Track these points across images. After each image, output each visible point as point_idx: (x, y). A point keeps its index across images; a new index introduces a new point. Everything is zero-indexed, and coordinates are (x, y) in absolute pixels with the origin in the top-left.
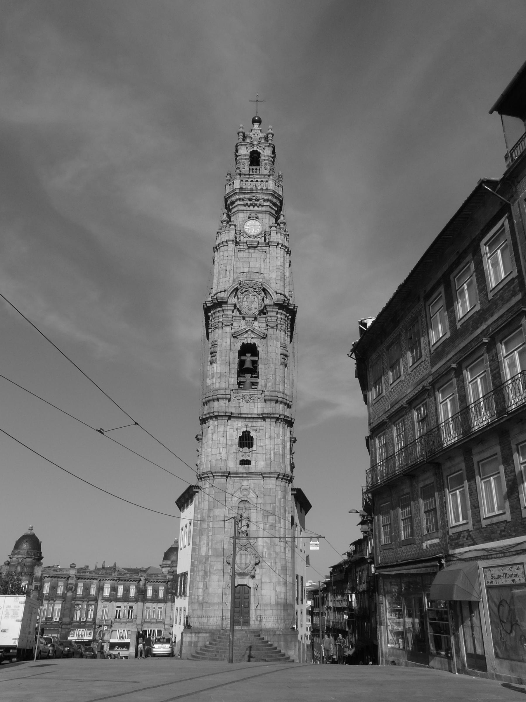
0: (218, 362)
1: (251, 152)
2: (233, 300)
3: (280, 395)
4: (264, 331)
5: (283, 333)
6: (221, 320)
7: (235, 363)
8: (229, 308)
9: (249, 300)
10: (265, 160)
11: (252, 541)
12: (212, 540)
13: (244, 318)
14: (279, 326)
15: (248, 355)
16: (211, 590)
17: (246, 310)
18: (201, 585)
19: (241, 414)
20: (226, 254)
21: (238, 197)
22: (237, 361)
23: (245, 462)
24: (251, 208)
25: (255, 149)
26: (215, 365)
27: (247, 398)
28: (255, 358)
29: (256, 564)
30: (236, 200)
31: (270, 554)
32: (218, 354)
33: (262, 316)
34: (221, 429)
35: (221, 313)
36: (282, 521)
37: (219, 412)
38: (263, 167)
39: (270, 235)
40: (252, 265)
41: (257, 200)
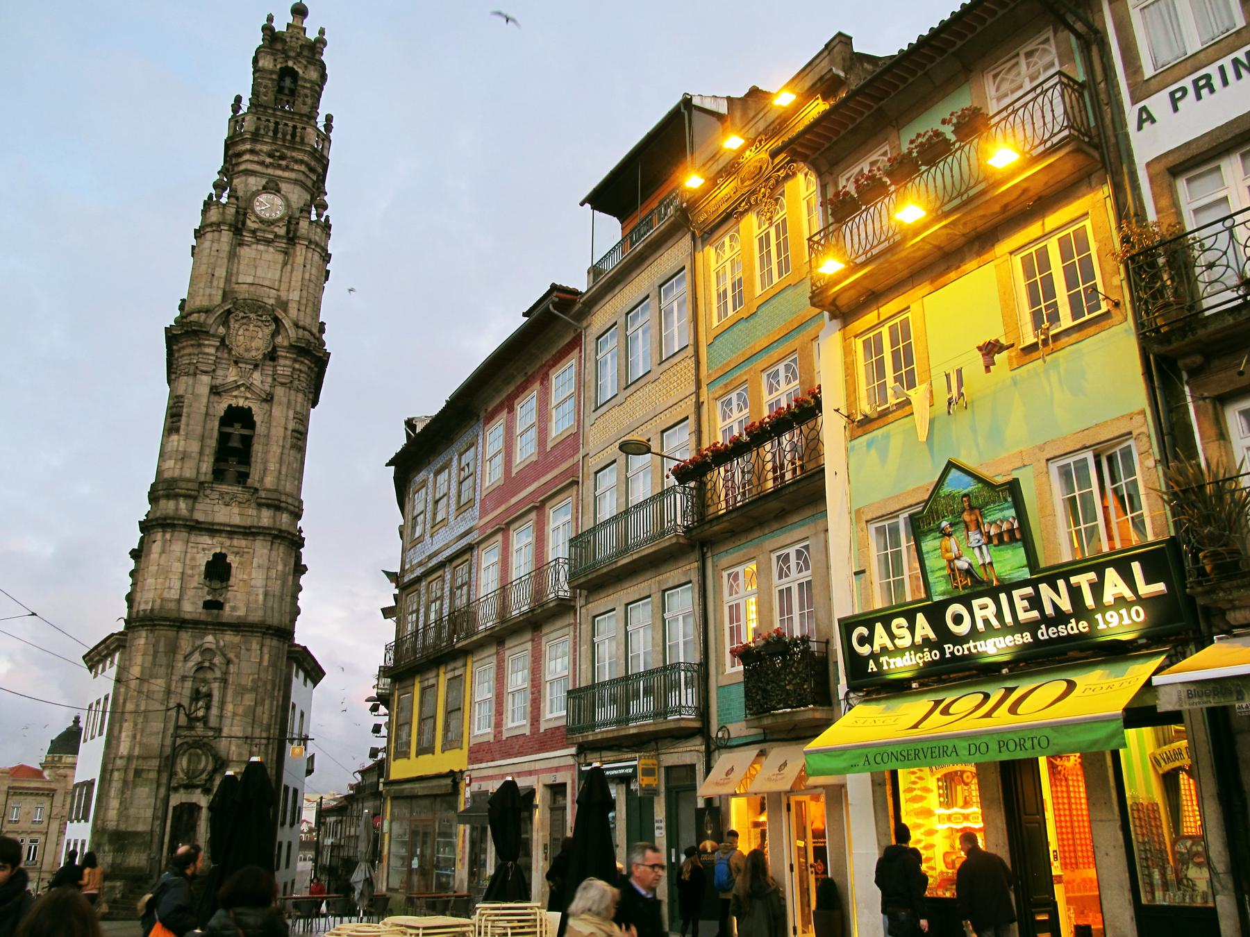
0: (182, 432)
2: (222, 330)
3: (283, 498)
4: (267, 388)
5: (301, 395)
7: (211, 438)
9: (247, 333)
12: (143, 731)
13: (236, 363)
14: (296, 382)
15: (238, 426)
16: (132, 811)
18: (114, 803)
19: (213, 524)
20: (215, 246)
21: (248, 147)
22: (216, 434)
25: (290, 64)
26: (175, 437)
27: (227, 498)
28: (246, 432)
30: (244, 152)
31: (240, 755)
32: (184, 420)
33: (268, 363)
34: (177, 547)
36: (267, 702)
38: (300, 100)
40: (260, 273)
41: (283, 157)
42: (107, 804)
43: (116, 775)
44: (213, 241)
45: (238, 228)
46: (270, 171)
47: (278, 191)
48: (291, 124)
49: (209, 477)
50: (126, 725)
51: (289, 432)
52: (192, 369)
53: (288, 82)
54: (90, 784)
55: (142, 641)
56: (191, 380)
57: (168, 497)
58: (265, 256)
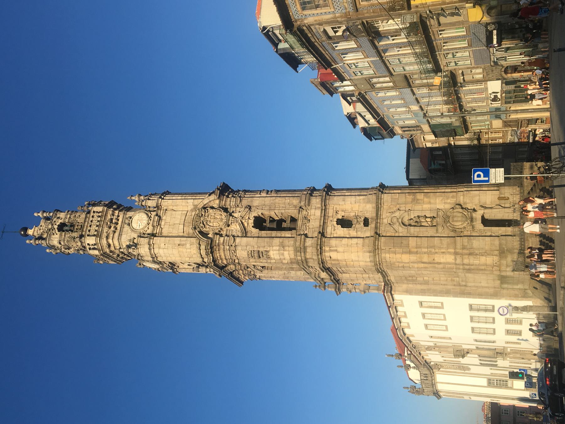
0: (268, 249)
1: (59, 231)
2: (210, 236)
6: (228, 247)
8: (217, 239)
10: (70, 217)
11: (441, 213)
13: (229, 226)
17: (221, 224)
18: (483, 259)
19: (320, 226)
20: (162, 245)
21: (105, 239)
23: (366, 222)
25: (56, 227)
26: (271, 254)
29: (462, 208)
31: (453, 197)
32: (261, 249)
35: (222, 247)
37: (317, 245)
39: (149, 207)
42: (483, 265)
43: (466, 261)
44: (159, 248)
45: (153, 235)
46: (119, 228)
47: (131, 218)
48: (91, 219)
49: (294, 231)
50: (437, 260)
51: (268, 195)
52: (233, 248)
54: (471, 308)
55: (388, 255)
56: (239, 248)
57: (305, 252)
58: (168, 220)
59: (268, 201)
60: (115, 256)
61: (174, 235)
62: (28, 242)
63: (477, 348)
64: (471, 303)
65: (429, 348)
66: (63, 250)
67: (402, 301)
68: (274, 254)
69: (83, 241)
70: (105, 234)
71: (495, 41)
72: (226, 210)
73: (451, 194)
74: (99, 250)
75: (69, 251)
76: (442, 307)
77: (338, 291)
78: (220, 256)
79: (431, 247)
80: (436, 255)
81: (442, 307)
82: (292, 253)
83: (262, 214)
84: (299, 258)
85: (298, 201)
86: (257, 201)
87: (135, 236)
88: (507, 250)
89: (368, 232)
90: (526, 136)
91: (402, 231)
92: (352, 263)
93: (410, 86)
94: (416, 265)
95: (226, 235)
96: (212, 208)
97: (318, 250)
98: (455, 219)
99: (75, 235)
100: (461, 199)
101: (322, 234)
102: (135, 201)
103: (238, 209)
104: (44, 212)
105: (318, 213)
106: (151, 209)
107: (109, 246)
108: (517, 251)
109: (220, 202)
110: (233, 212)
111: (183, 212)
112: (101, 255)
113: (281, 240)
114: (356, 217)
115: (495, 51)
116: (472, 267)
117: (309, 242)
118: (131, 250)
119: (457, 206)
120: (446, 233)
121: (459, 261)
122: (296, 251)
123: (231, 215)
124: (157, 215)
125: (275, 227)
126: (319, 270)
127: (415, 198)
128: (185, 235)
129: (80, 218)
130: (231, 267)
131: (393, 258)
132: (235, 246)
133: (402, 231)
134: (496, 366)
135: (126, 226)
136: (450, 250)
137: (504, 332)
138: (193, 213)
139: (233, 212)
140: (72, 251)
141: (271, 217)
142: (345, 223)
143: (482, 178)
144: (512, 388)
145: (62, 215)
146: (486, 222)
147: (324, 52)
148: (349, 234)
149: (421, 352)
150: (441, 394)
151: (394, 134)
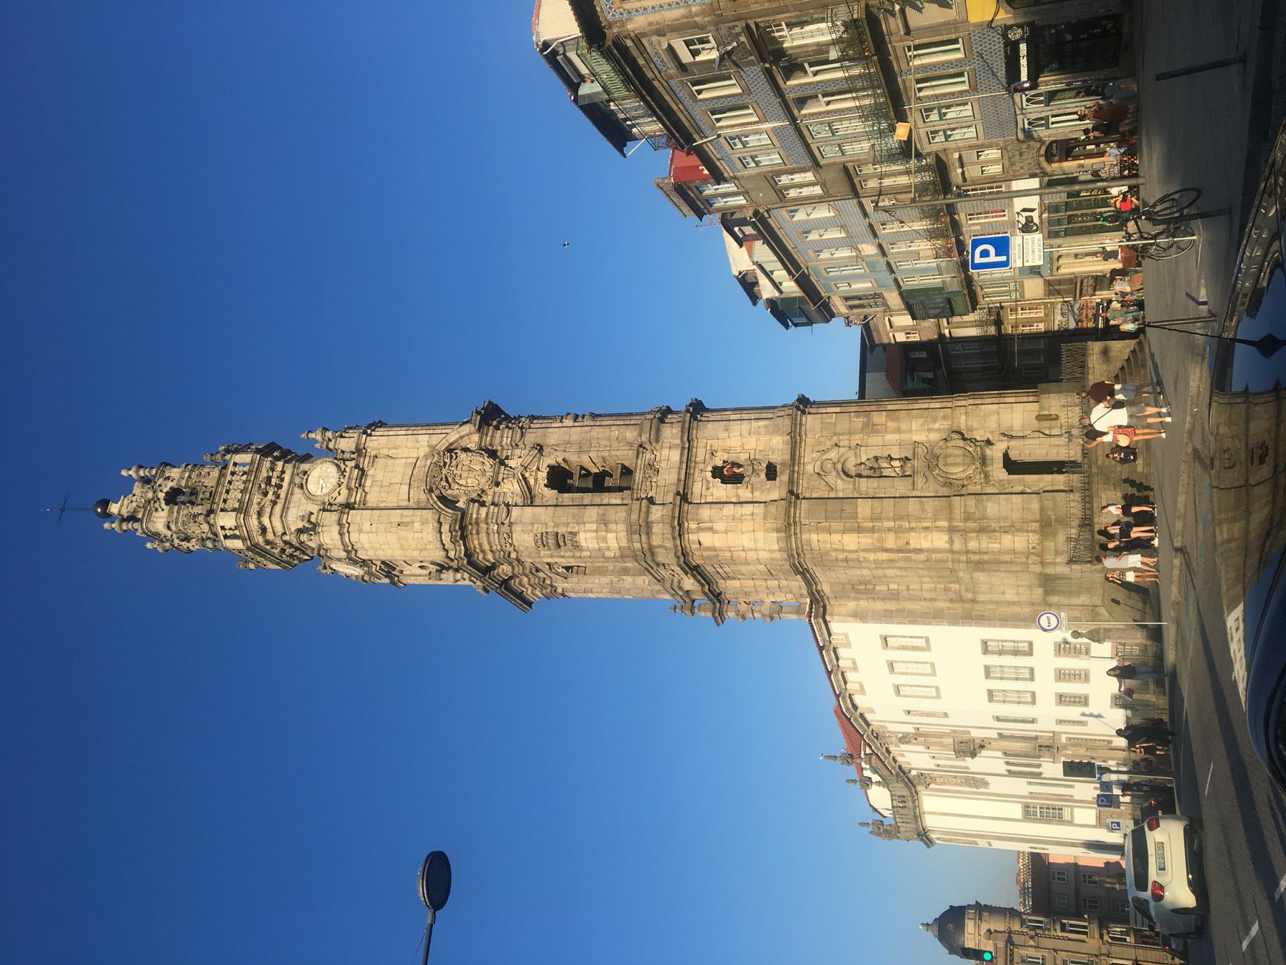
2: (460, 505)
10: (189, 477)
11: (920, 451)
13: (497, 484)
17: (483, 480)
18: (1007, 541)
19: (679, 480)
20: (366, 526)
21: (255, 516)
23: (771, 473)
24: (283, 493)
25: (161, 495)
29: (964, 439)
31: (944, 418)
32: (562, 530)
35: (483, 526)
37: (673, 517)
39: (343, 452)
43: (973, 545)
44: (360, 531)
45: (349, 506)
46: (283, 496)
47: (305, 473)
48: (229, 477)
49: (627, 493)
50: (913, 544)
52: (505, 529)
53: (182, 498)
55: (814, 537)
57: (648, 534)
58: (379, 476)
59: (576, 433)
60: (276, 551)
61: (389, 505)
62: (106, 526)
63: (1000, 735)
64: (986, 637)
65: (905, 739)
66: (176, 542)
67: (846, 636)
68: (587, 539)
69: (212, 522)
70: (255, 508)
71: (1024, 76)
72: (492, 454)
73: (942, 413)
74: (244, 540)
75: (189, 545)
76: (927, 648)
77: (719, 617)
78: (480, 545)
79: (901, 518)
80: (913, 534)
81: (927, 648)
82: (623, 535)
83: (564, 460)
84: (637, 545)
85: (636, 433)
86: (554, 435)
87: (315, 509)
88: (1056, 520)
89: (775, 491)
90: (1090, 315)
91: (842, 487)
92: (743, 554)
93: (856, 195)
94: (871, 556)
95: (493, 504)
96: (466, 450)
97: (673, 528)
98: (950, 460)
99: (197, 510)
100: (962, 422)
101: (684, 497)
102: (316, 441)
103: (517, 452)
104: (140, 467)
105: (675, 456)
106: (347, 456)
107: (264, 530)
108: (1077, 522)
109: (481, 438)
110: (507, 458)
111: (410, 461)
112: (248, 549)
113: (601, 510)
114: (752, 462)
115: (1025, 103)
116: (986, 557)
117: (656, 513)
118: (304, 537)
119: (955, 436)
120: (933, 488)
121: (958, 545)
122: (631, 531)
123: (502, 463)
124: (357, 466)
125: (591, 486)
126: (678, 569)
127: (868, 422)
128: (412, 504)
129: (209, 477)
130: (505, 570)
131: (825, 542)
132: (511, 524)
133: (842, 487)
134: (1039, 775)
135: (297, 490)
136: (938, 524)
137: (1053, 699)
138: (428, 462)
139: (507, 458)
140: (193, 545)
141: (582, 468)
142: (729, 474)
143: (993, 258)
144: (1070, 823)
145: (175, 473)
146: (1012, 466)
147: (675, 107)
148: (738, 496)
149: (891, 749)
150: (933, 836)
151: (833, 315)
